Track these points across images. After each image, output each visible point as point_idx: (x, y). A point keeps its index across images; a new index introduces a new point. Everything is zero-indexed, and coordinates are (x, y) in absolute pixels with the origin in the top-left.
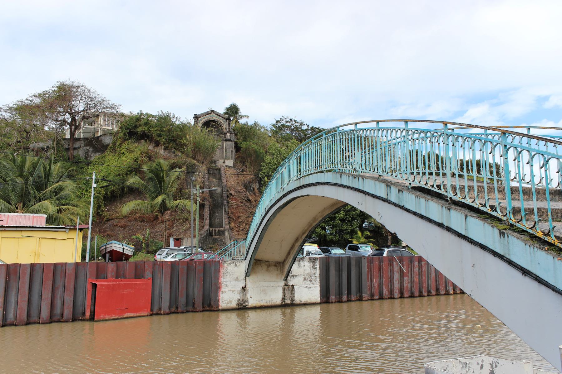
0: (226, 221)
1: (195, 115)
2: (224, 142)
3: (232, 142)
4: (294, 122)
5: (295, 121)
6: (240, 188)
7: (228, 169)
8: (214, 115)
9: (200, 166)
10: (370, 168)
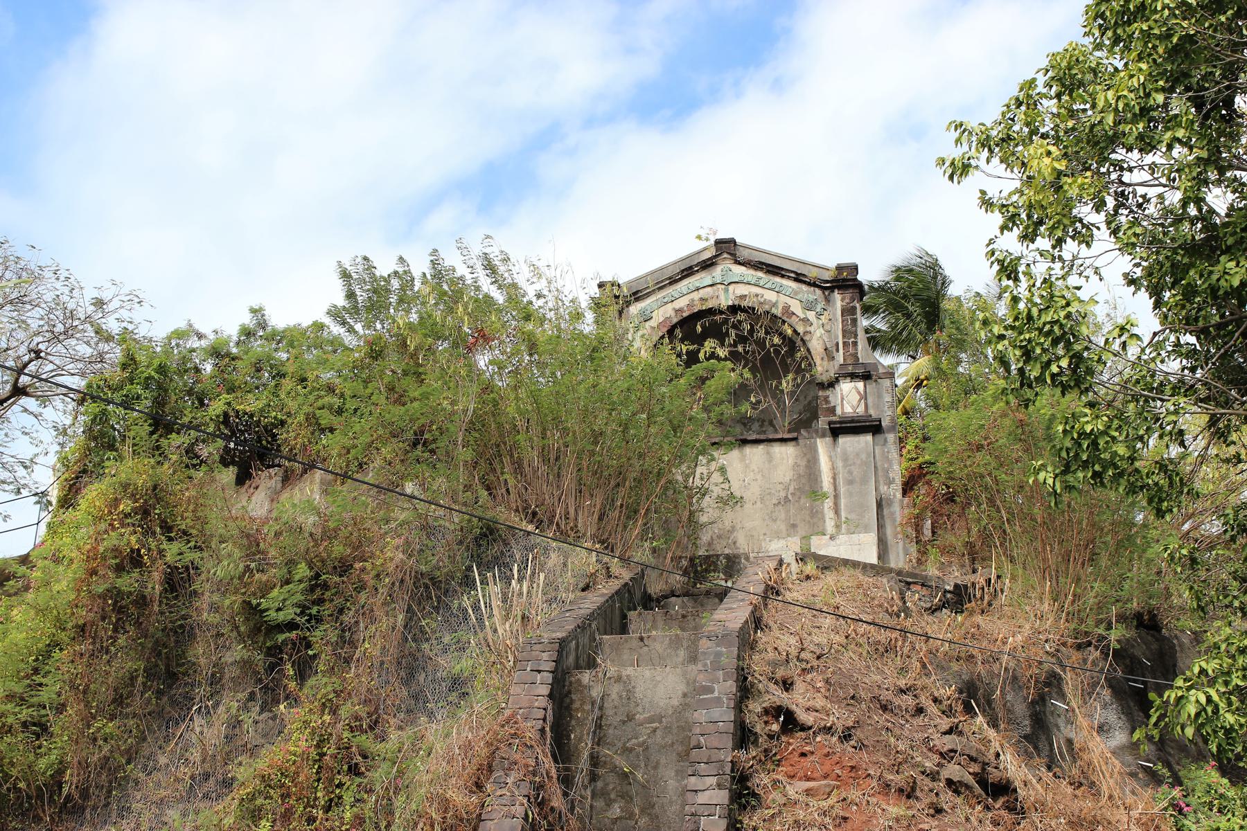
2: (822, 446)
3: (880, 437)
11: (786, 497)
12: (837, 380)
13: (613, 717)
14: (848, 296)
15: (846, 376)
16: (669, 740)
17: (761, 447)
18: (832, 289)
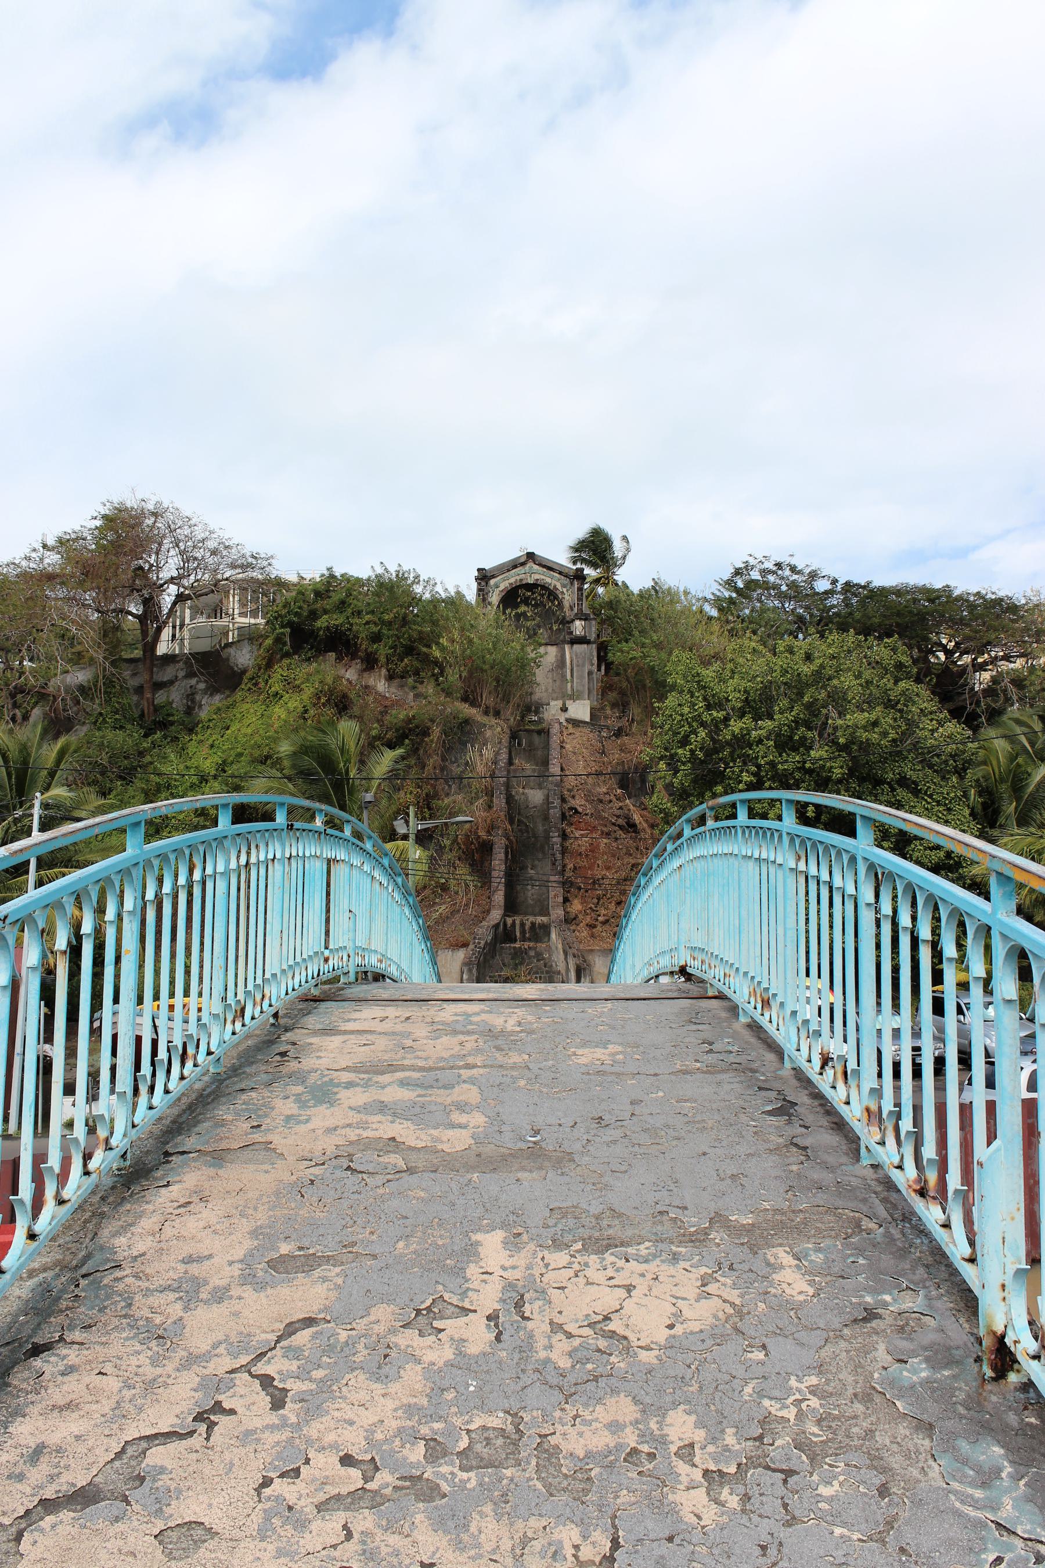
0: (556, 896)
1: (479, 570)
2: (567, 647)
4: (787, 572)
5: (793, 569)
6: (604, 790)
7: (571, 730)
8: (536, 567)
9: (485, 725)
10: (746, 857)
13: (522, 807)
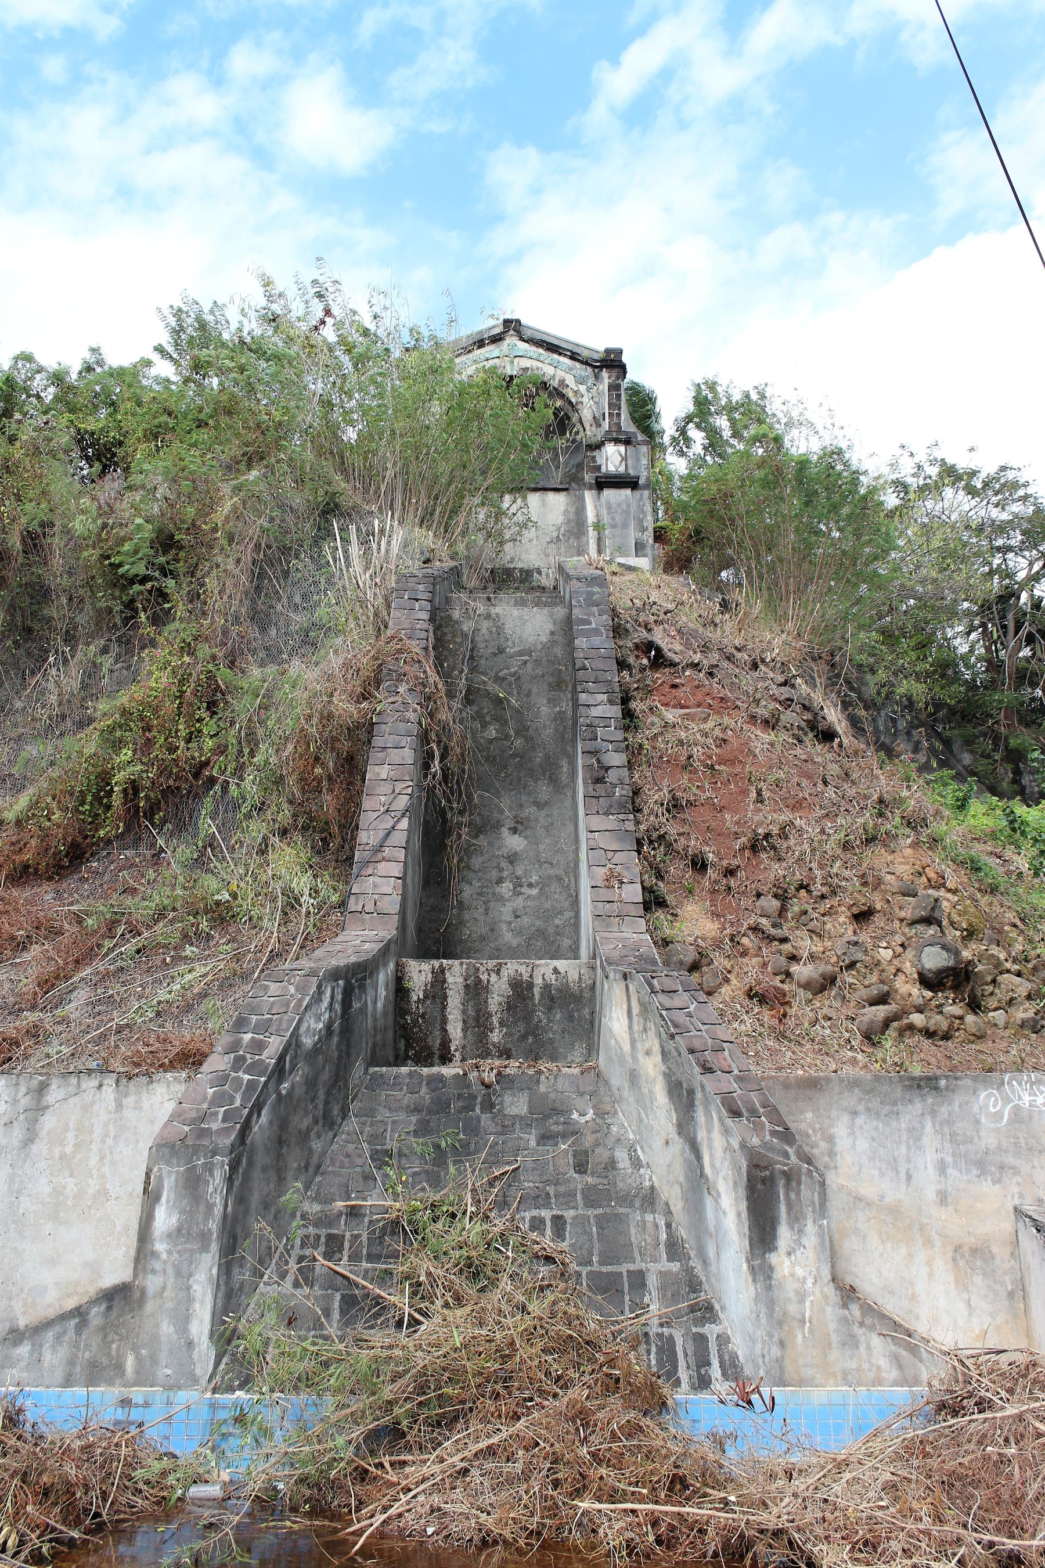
0: (614, 879)
2: (589, 496)
3: (637, 493)
11: (558, 537)
12: (603, 443)
13: (483, 650)
14: (614, 375)
15: (610, 440)
16: (539, 671)
17: (538, 494)
18: (601, 368)
